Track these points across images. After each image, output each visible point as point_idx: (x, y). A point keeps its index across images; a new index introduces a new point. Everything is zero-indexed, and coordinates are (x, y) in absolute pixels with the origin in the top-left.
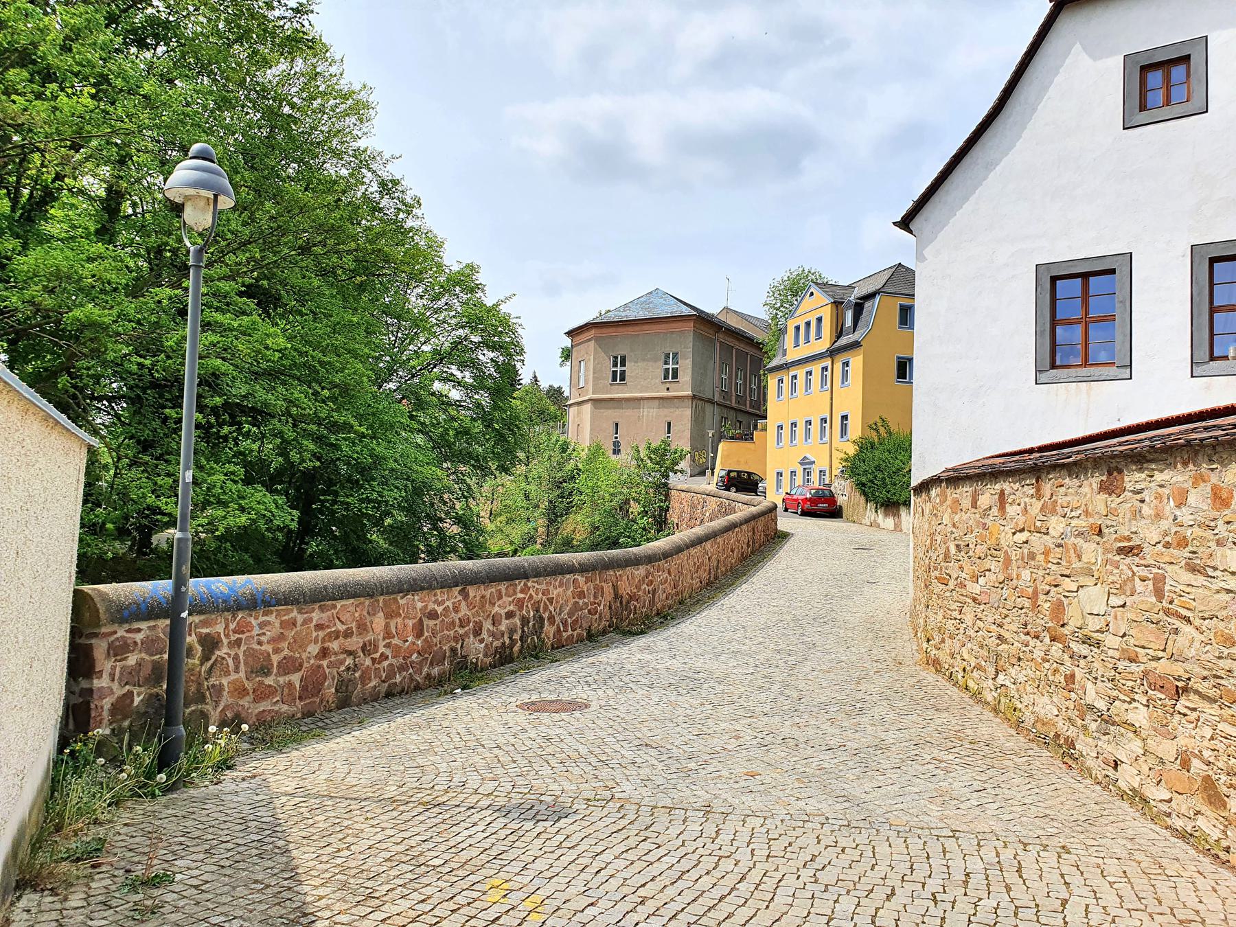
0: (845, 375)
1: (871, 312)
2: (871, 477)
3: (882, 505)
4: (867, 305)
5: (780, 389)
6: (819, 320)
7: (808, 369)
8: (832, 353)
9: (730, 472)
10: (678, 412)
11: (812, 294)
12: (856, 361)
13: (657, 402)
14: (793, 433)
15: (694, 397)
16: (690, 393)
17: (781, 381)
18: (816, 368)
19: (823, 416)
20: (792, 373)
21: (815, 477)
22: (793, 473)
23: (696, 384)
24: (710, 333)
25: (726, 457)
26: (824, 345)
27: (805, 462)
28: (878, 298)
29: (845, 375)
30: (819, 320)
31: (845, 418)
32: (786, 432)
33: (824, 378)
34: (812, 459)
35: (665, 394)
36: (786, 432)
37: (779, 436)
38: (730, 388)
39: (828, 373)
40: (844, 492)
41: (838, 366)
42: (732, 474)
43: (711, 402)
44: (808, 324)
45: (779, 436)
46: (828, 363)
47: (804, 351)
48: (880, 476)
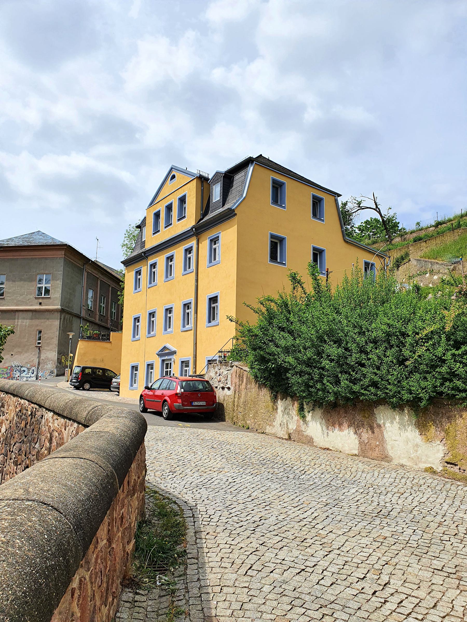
0: (213, 253)
1: (244, 182)
2: (309, 353)
3: (318, 404)
4: (238, 177)
5: (137, 282)
6: (182, 200)
7: (169, 254)
8: (198, 231)
9: (84, 369)
10: (48, 322)
11: (174, 177)
12: (228, 235)
13: (30, 314)
14: (151, 324)
15: (62, 311)
16: (59, 307)
17: (138, 273)
18: (178, 252)
19: (186, 301)
20: (150, 262)
21: (176, 370)
22: (150, 366)
23: (67, 299)
24: (79, 263)
25: (83, 355)
26: (190, 222)
27: (165, 353)
28: (251, 169)
29: (213, 253)
30: (182, 200)
31: (213, 300)
32: (143, 324)
33: (187, 262)
34: (173, 349)
35: (38, 307)
36: (143, 324)
37: (136, 329)
38: (95, 309)
39: (193, 255)
40: (231, 385)
41: (205, 245)
42: (87, 371)
43: (78, 317)
44: (169, 208)
45: (136, 329)
46: (193, 243)
47: (166, 234)
48: (334, 350)
